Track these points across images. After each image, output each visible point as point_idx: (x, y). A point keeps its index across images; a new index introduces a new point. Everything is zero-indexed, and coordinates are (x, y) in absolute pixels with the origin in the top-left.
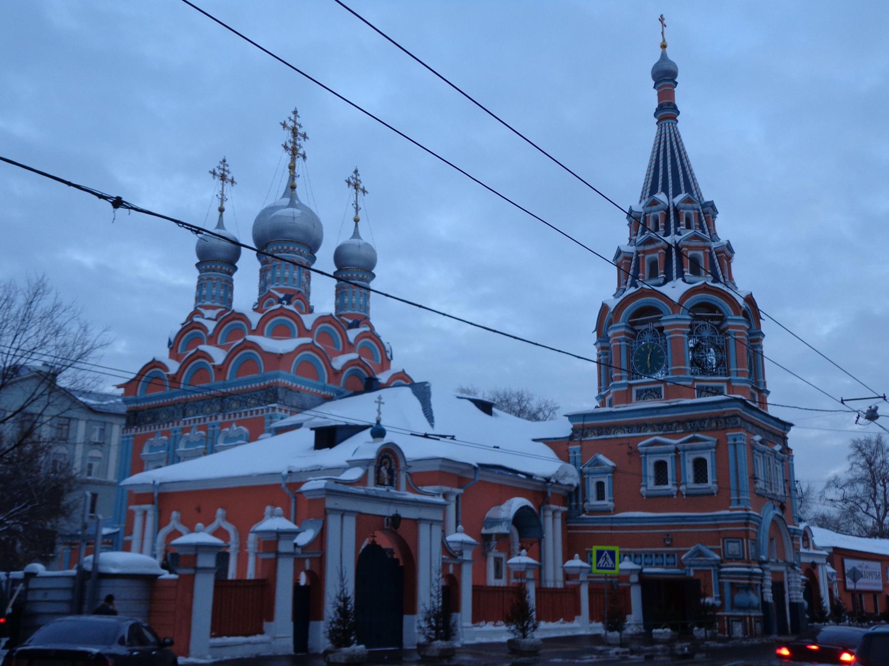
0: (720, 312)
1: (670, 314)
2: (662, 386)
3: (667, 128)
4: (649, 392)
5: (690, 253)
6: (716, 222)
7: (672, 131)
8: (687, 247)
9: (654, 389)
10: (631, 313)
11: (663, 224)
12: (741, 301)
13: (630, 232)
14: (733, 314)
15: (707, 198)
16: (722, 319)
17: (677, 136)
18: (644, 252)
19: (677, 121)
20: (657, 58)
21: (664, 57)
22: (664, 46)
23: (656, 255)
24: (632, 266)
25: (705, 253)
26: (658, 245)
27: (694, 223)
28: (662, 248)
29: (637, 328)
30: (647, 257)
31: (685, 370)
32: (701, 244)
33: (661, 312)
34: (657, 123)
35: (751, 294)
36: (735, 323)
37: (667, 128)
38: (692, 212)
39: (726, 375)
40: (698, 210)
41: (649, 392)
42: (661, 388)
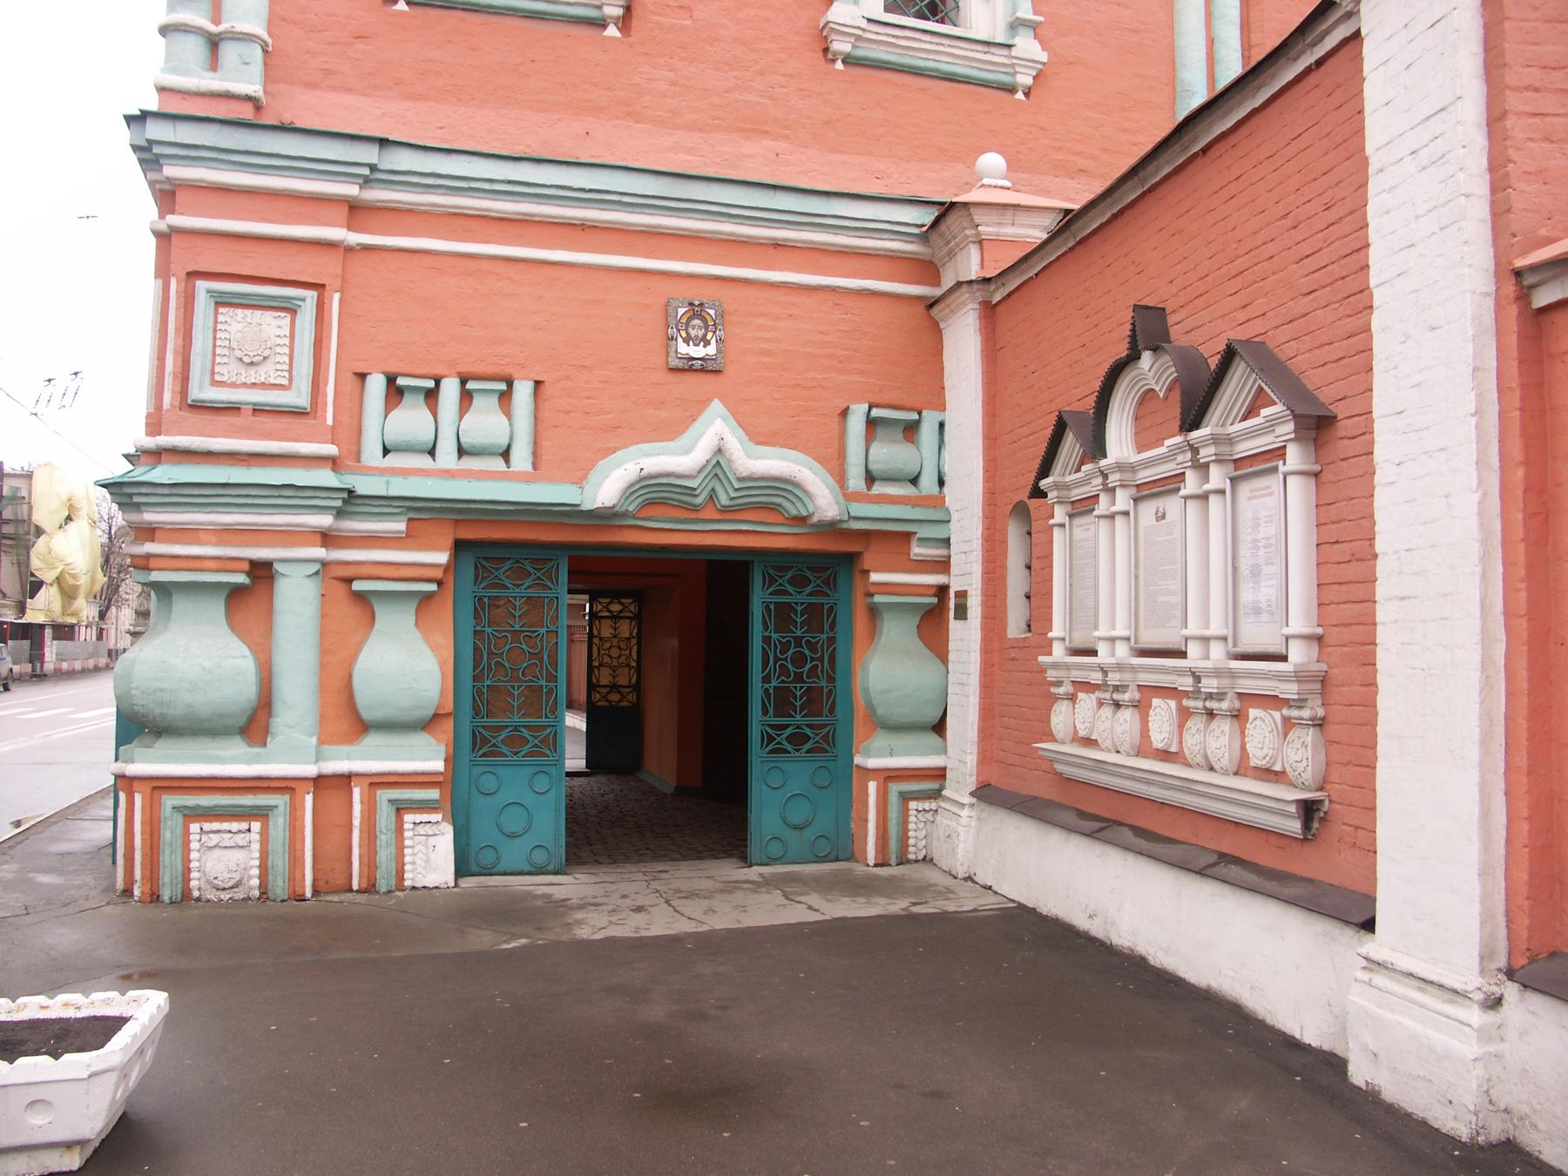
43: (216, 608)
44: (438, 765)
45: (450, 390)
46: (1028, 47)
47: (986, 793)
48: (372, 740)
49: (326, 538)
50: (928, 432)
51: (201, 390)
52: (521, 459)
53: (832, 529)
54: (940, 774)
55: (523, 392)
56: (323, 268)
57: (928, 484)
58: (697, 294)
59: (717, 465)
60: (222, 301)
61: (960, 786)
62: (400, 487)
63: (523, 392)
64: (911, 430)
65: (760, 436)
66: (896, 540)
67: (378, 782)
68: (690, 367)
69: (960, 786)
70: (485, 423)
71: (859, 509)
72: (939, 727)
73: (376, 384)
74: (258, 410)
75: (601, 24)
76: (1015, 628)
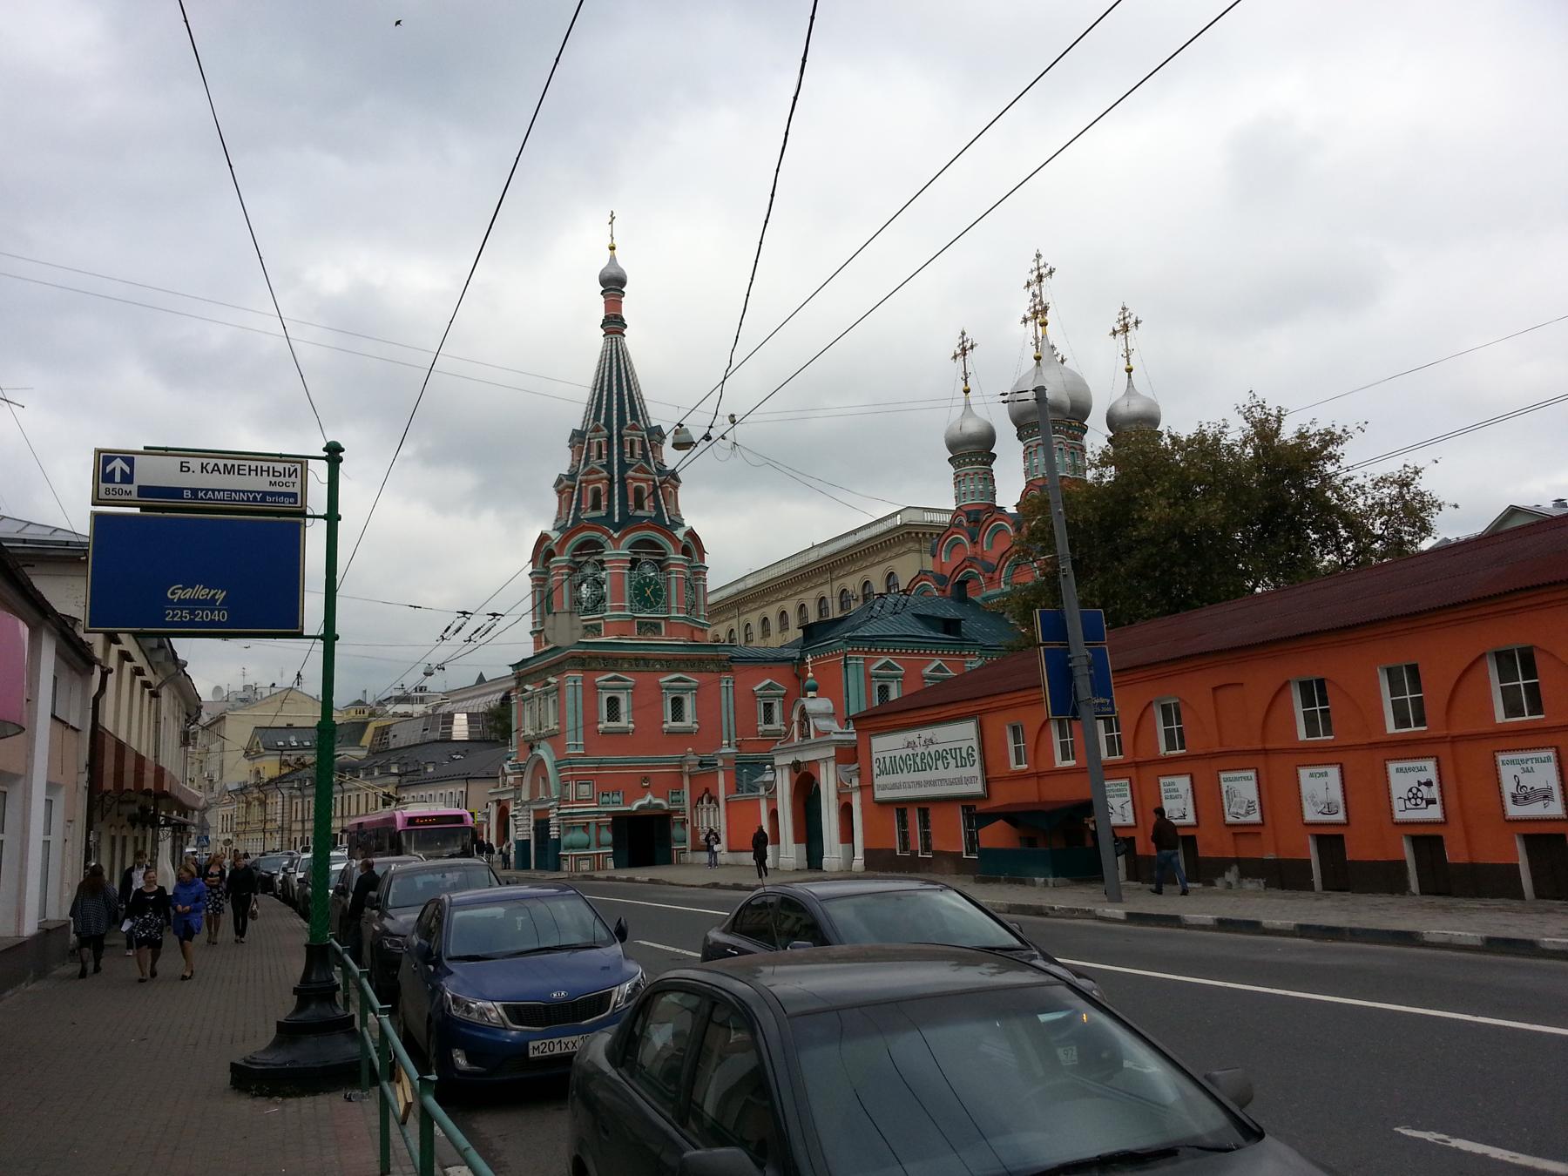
0: (659, 547)
1: (611, 550)
2: (602, 621)
3: (614, 343)
4: (589, 628)
5: (635, 484)
6: (663, 448)
7: (620, 348)
8: (632, 478)
9: (595, 624)
10: (573, 547)
11: (606, 452)
12: (680, 533)
13: (573, 456)
14: (673, 552)
15: (653, 425)
16: (663, 554)
17: (625, 353)
18: (586, 481)
19: (624, 336)
20: (605, 262)
21: (613, 259)
22: (612, 248)
23: (600, 485)
24: (575, 497)
25: (648, 485)
26: (601, 475)
27: (638, 451)
28: (606, 478)
29: (578, 559)
30: (591, 487)
31: (624, 606)
32: (643, 476)
33: (604, 548)
34: (604, 336)
35: (692, 528)
36: (675, 556)
37: (614, 343)
38: (635, 438)
39: (665, 612)
40: (643, 437)
41: (589, 628)
42: (600, 624)
43: (581, 829)
44: (612, 851)
45: (611, 794)
46: (696, 726)
47: (692, 850)
48: (602, 848)
49: (596, 818)
50: (681, 793)
51: (579, 798)
52: (621, 803)
53: (667, 810)
54: (685, 849)
55: (621, 794)
56: (593, 777)
57: (681, 802)
58: (646, 775)
59: (650, 802)
60: (580, 784)
61: (689, 850)
62: (606, 809)
63: (621, 794)
64: (679, 793)
65: (656, 797)
66: (676, 812)
67: (602, 853)
68: (646, 787)
69: (689, 850)
70: (616, 798)
71: (671, 807)
72: (685, 842)
73: (601, 794)
74: (587, 800)
75: (628, 733)
76: (695, 825)
